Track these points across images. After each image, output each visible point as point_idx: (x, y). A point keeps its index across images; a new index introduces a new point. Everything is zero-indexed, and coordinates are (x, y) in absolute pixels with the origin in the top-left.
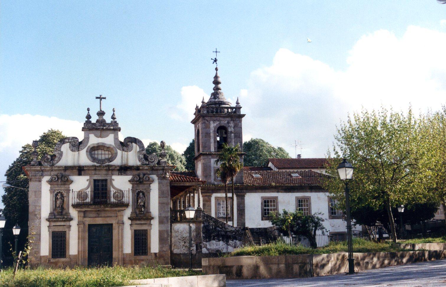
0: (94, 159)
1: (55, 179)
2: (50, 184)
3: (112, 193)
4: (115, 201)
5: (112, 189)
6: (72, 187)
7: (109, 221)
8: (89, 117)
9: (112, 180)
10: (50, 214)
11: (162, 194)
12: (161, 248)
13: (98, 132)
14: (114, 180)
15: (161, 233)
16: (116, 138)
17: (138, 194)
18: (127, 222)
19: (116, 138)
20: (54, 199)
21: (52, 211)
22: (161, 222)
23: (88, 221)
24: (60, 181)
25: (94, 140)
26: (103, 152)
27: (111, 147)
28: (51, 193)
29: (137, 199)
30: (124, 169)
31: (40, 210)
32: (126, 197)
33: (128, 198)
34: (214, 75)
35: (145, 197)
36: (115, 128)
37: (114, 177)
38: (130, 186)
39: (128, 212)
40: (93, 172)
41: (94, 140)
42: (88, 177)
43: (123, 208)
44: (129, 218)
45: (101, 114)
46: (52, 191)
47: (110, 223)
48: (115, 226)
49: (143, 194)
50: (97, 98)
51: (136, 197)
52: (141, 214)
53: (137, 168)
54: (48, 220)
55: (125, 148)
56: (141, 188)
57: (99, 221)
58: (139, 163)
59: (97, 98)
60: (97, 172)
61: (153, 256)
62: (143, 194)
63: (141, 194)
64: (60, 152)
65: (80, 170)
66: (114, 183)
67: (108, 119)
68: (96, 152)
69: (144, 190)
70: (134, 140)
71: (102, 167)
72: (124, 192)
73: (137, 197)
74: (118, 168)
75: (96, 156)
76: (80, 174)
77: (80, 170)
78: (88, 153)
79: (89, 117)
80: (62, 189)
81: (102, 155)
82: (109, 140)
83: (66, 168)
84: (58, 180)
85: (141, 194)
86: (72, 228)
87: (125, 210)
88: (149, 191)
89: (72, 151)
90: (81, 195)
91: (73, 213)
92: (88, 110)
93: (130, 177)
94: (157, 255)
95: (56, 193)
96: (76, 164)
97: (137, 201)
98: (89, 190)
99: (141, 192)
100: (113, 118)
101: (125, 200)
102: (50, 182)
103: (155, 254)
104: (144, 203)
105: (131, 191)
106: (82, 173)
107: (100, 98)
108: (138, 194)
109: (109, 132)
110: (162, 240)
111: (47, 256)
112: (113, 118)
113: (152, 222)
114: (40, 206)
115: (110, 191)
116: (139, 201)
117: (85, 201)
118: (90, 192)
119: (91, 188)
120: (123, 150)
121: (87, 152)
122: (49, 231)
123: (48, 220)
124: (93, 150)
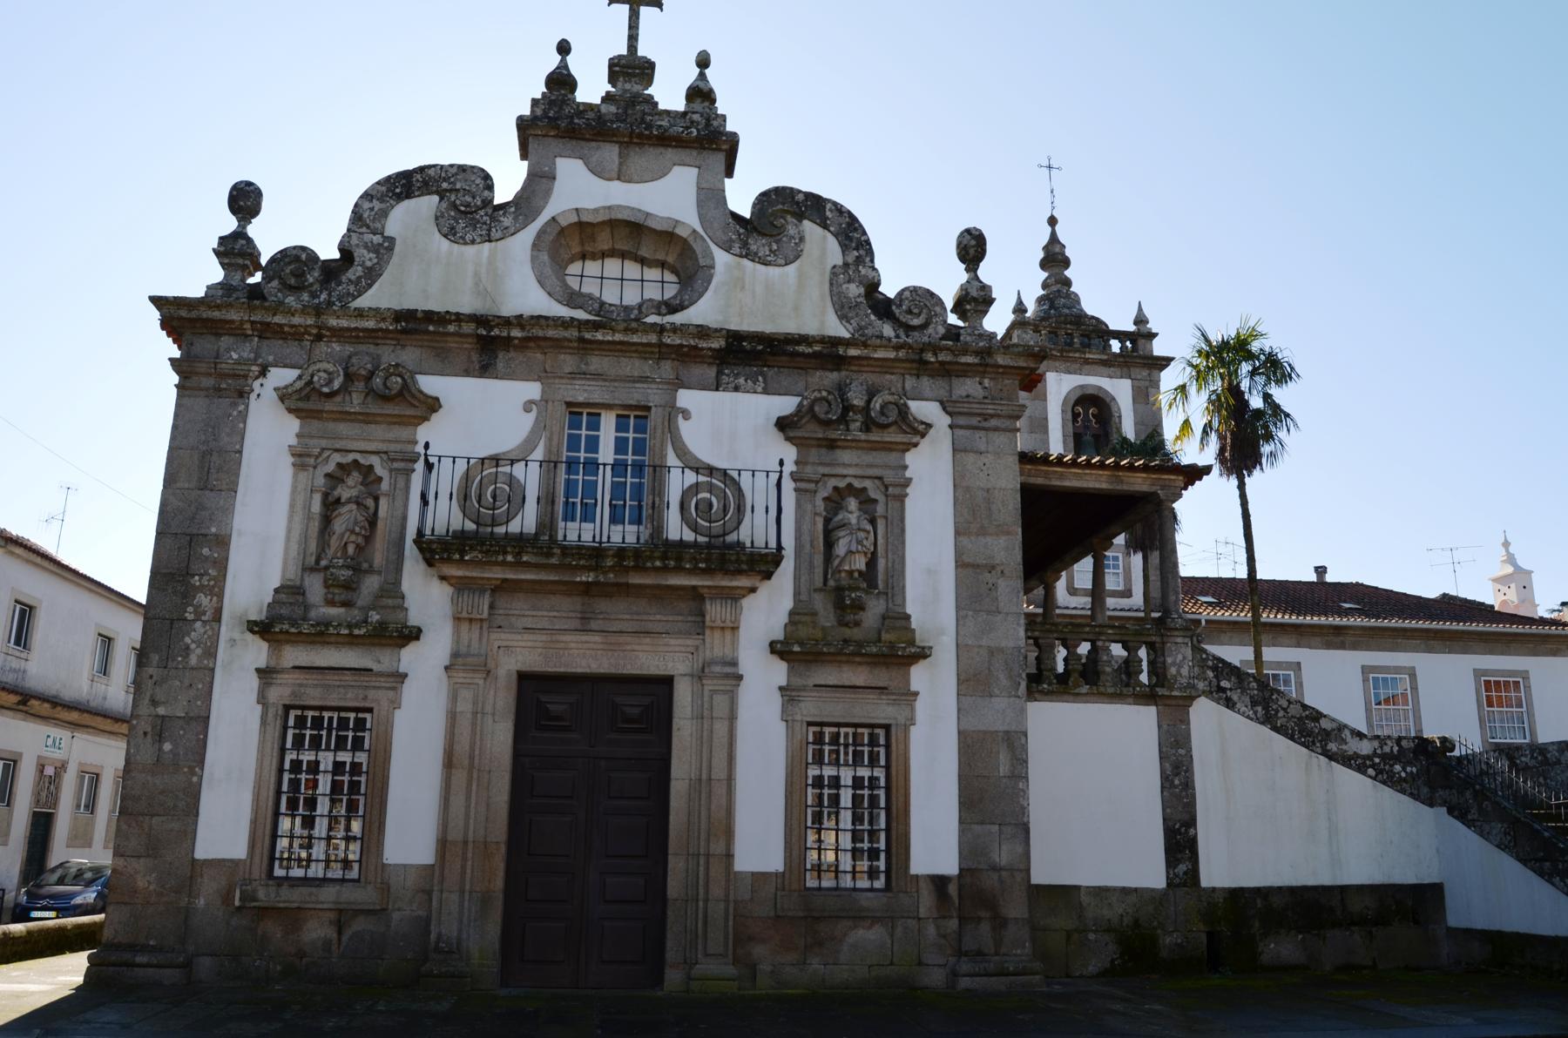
1: (330, 382)
4: (689, 536)
6: (436, 435)
7: (646, 659)
8: (561, 81)
9: (674, 413)
10: (277, 591)
11: (970, 517)
12: (969, 849)
13: (610, 153)
14: (686, 414)
15: (972, 747)
16: (711, 197)
18: (762, 677)
19: (711, 197)
20: (316, 507)
21: (293, 573)
22: (972, 683)
25: (580, 187)
26: (632, 270)
27: (682, 232)
30: (744, 356)
31: (222, 565)
32: (760, 510)
34: (1045, 239)
35: (873, 521)
36: (705, 137)
37: (685, 398)
39: (767, 610)
40: (568, 362)
41: (580, 187)
42: (533, 390)
43: (743, 582)
44: (778, 649)
45: (631, 70)
46: (302, 458)
48: (683, 695)
49: (867, 502)
51: (820, 526)
52: (852, 630)
53: (828, 354)
56: (851, 464)
57: (585, 654)
58: (836, 328)
60: (597, 363)
61: (926, 902)
62: (867, 502)
63: (852, 504)
64: (377, 239)
65: (489, 343)
66: (685, 428)
69: (867, 484)
70: (813, 207)
72: (745, 481)
73: (827, 521)
74: (718, 343)
76: (485, 370)
77: (489, 343)
78: (545, 257)
79: (561, 81)
80: (367, 442)
82: (669, 195)
84: (344, 389)
85: (852, 504)
86: (409, 691)
87: (753, 590)
88: (897, 491)
89: (450, 234)
90: (486, 482)
91: (426, 596)
92: (564, 48)
93: (786, 405)
94: (952, 889)
95: (330, 467)
96: (466, 303)
97: (829, 544)
100: (700, 94)
101: (755, 531)
102: (300, 401)
103: (939, 882)
104: (872, 563)
105: (788, 486)
106: (500, 365)
108: (835, 502)
109: (670, 154)
111: (235, 863)
112: (700, 94)
113: (918, 676)
114: (223, 542)
116: (841, 549)
117: (501, 530)
120: (748, 255)
121: (536, 246)
122: (262, 699)
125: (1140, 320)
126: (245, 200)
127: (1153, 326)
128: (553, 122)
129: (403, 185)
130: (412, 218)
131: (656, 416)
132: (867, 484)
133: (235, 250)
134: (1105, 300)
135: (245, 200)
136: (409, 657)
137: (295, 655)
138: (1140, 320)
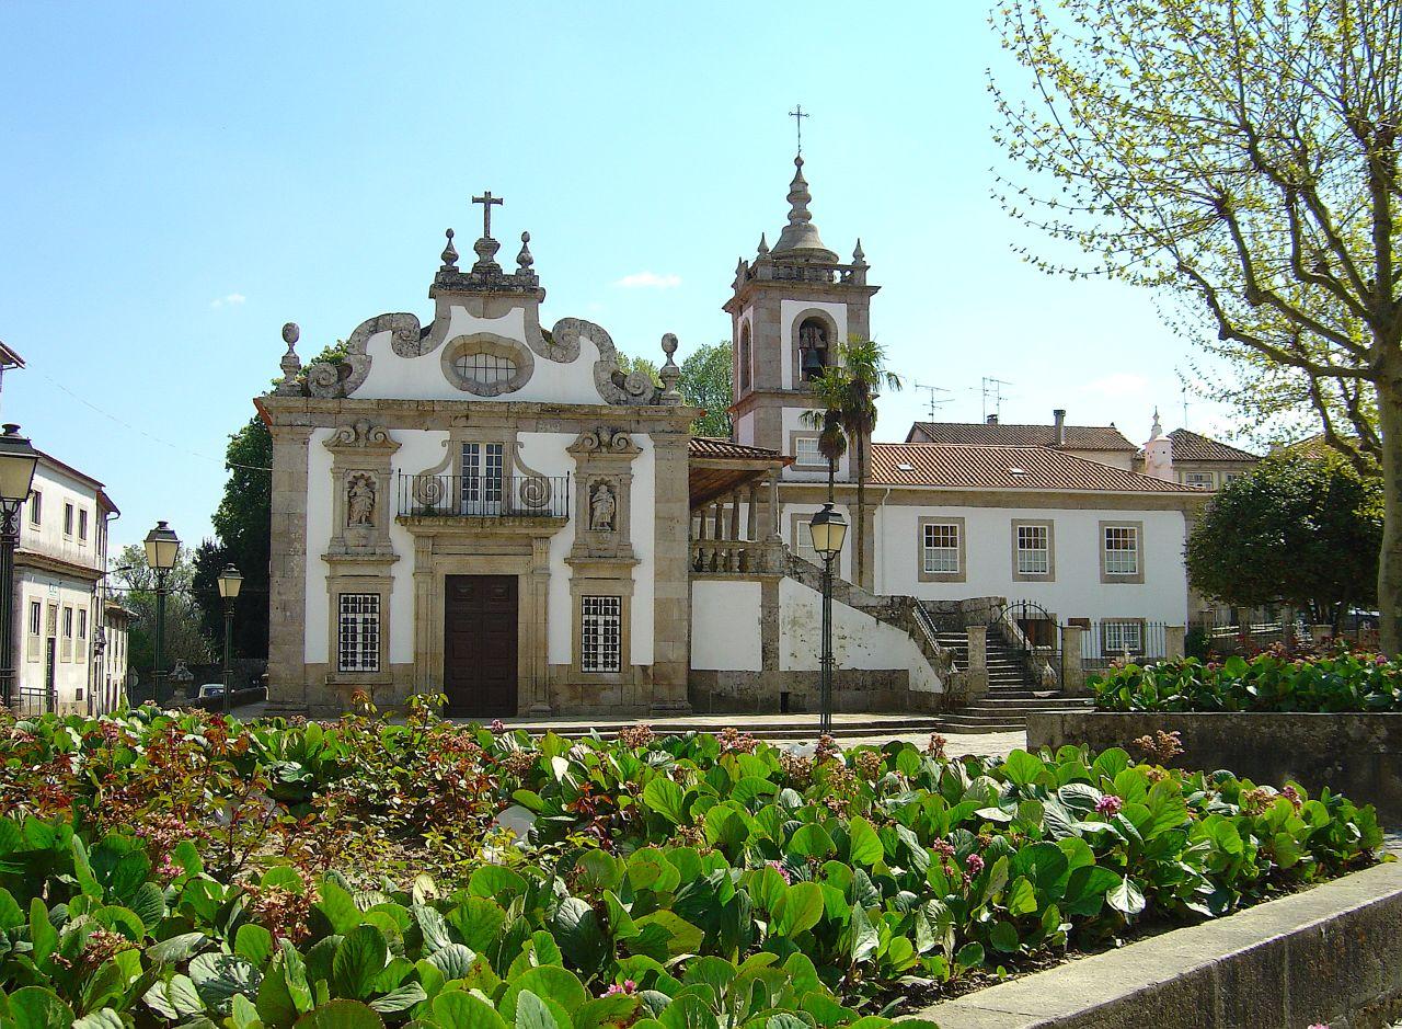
0: (464, 383)
2: (333, 452)
3: (517, 484)
4: (525, 507)
5: (517, 472)
6: (397, 461)
7: (505, 567)
8: (450, 256)
9: (515, 445)
13: (478, 302)
15: (661, 606)
17: (595, 490)
19: (532, 322)
23: (450, 566)
24: (362, 442)
26: (491, 362)
28: (336, 479)
29: (591, 504)
30: (552, 415)
32: (558, 497)
33: (565, 497)
36: (526, 288)
37: (522, 436)
38: (570, 464)
41: (464, 323)
42: (446, 435)
45: (487, 246)
47: (507, 570)
50: (475, 200)
54: (329, 558)
55: (556, 351)
56: (603, 468)
57: (478, 566)
59: (475, 200)
61: (639, 675)
63: (604, 488)
65: (422, 413)
67: (507, 262)
68: (471, 361)
70: (584, 326)
71: (486, 408)
72: (551, 481)
73: (592, 497)
75: (470, 373)
79: (450, 256)
80: (365, 463)
81: (487, 370)
82: (509, 325)
83: (384, 405)
84: (356, 439)
85: (604, 488)
86: (396, 585)
88: (627, 479)
89: (399, 353)
90: (425, 480)
91: (401, 540)
92: (450, 234)
93: (570, 438)
94: (650, 672)
95: (351, 478)
98: (449, 471)
99: (603, 482)
100: (524, 260)
101: (556, 505)
102: (335, 446)
103: (644, 668)
104: (613, 517)
105: (572, 480)
107: (488, 201)
108: (595, 490)
110: (662, 630)
112: (524, 260)
114: (304, 517)
115: (510, 478)
118: (450, 479)
119: (454, 465)
122: (329, 590)
123: (329, 558)
124: (460, 355)
125: (858, 254)
126: (290, 334)
127: (868, 259)
128: (448, 284)
129: (375, 325)
130: (380, 344)
131: (506, 448)
132: (611, 478)
133: (289, 363)
134: (833, 235)
135: (290, 334)
136: (395, 570)
137: (342, 570)
138: (858, 254)
